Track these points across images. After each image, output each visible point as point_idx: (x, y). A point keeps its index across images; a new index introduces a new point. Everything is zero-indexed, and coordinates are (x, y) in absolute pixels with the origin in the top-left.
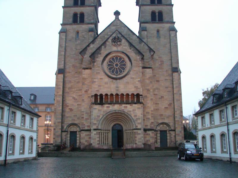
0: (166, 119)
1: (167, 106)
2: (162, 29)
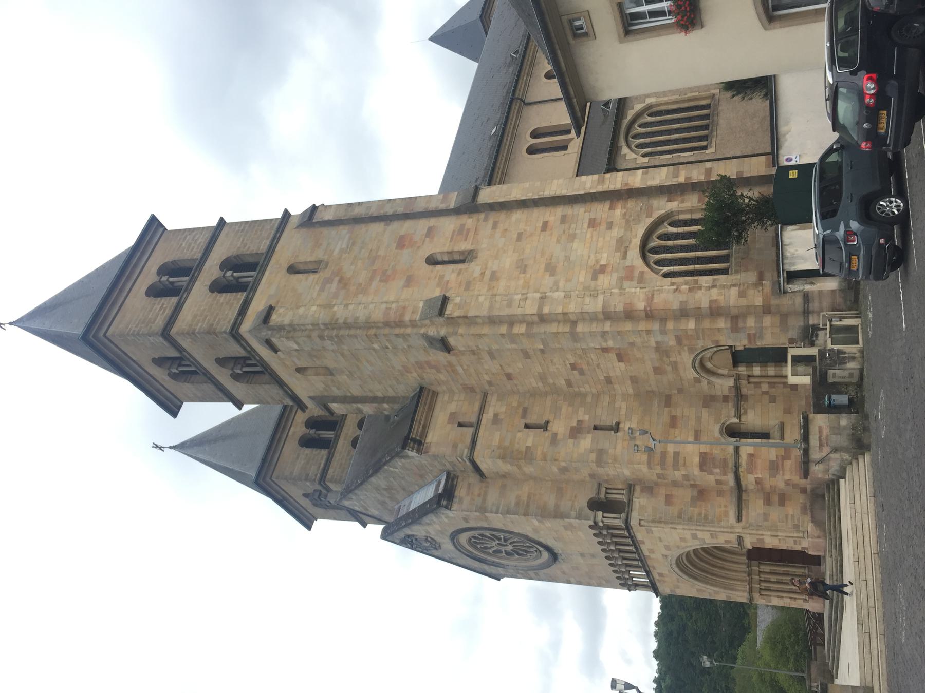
0: (673, 359)
1: (613, 356)
2: (287, 363)
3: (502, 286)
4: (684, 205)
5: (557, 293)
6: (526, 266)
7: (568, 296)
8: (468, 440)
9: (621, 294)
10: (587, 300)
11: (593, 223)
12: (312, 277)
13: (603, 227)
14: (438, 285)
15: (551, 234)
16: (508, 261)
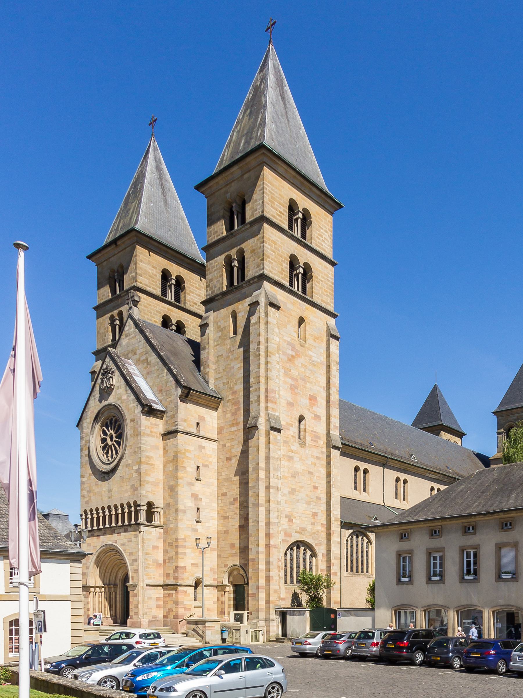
3: (285, 463)
4: (320, 562)
5: (280, 496)
6: (295, 477)
7: (278, 503)
8: (188, 430)
9: (278, 531)
10: (276, 514)
11: (315, 514)
12: (296, 335)
13: (312, 520)
14: (287, 423)
15: (311, 491)
16: (298, 466)
